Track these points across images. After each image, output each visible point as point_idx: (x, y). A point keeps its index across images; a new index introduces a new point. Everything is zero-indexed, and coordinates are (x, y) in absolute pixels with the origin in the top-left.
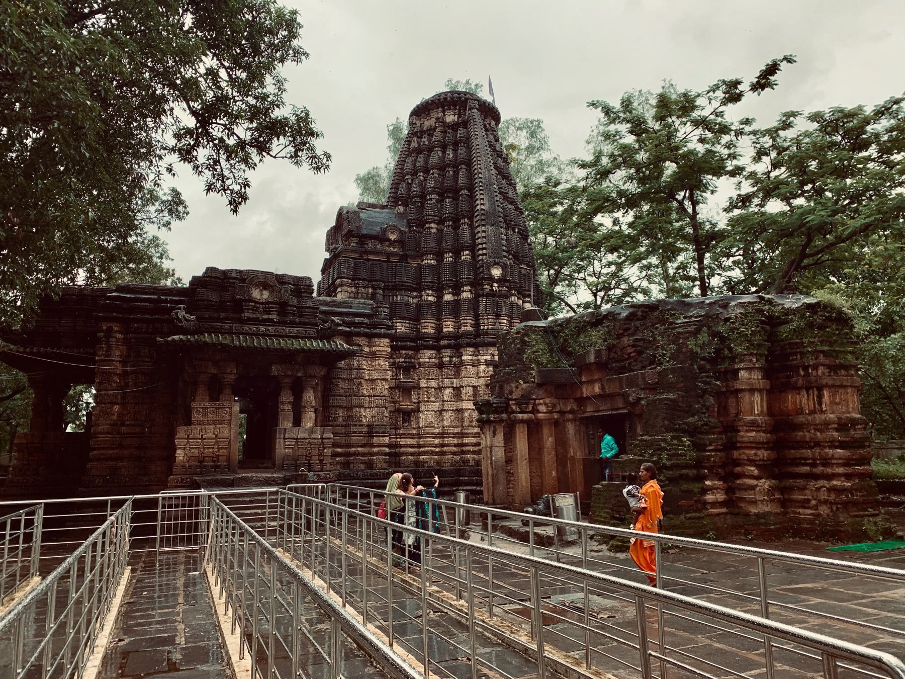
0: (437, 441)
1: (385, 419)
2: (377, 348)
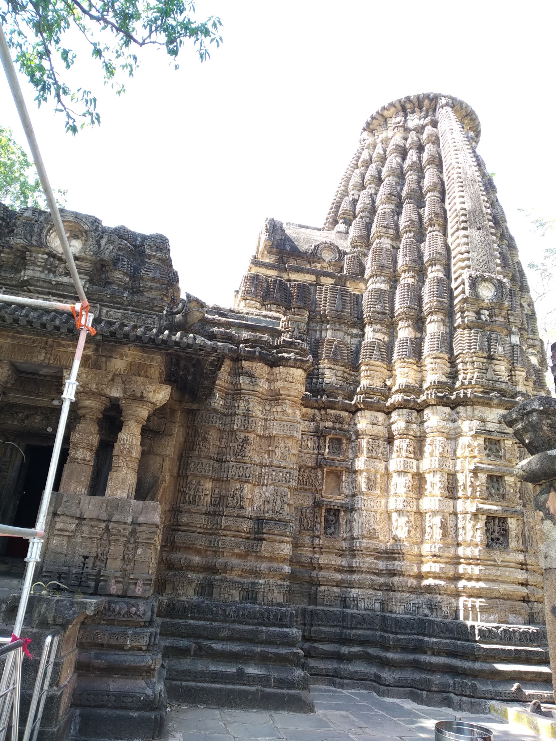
0: (381, 565)
1: (286, 508)
2: (281, 384)
